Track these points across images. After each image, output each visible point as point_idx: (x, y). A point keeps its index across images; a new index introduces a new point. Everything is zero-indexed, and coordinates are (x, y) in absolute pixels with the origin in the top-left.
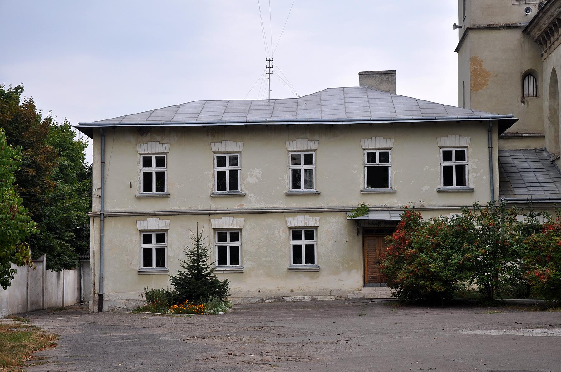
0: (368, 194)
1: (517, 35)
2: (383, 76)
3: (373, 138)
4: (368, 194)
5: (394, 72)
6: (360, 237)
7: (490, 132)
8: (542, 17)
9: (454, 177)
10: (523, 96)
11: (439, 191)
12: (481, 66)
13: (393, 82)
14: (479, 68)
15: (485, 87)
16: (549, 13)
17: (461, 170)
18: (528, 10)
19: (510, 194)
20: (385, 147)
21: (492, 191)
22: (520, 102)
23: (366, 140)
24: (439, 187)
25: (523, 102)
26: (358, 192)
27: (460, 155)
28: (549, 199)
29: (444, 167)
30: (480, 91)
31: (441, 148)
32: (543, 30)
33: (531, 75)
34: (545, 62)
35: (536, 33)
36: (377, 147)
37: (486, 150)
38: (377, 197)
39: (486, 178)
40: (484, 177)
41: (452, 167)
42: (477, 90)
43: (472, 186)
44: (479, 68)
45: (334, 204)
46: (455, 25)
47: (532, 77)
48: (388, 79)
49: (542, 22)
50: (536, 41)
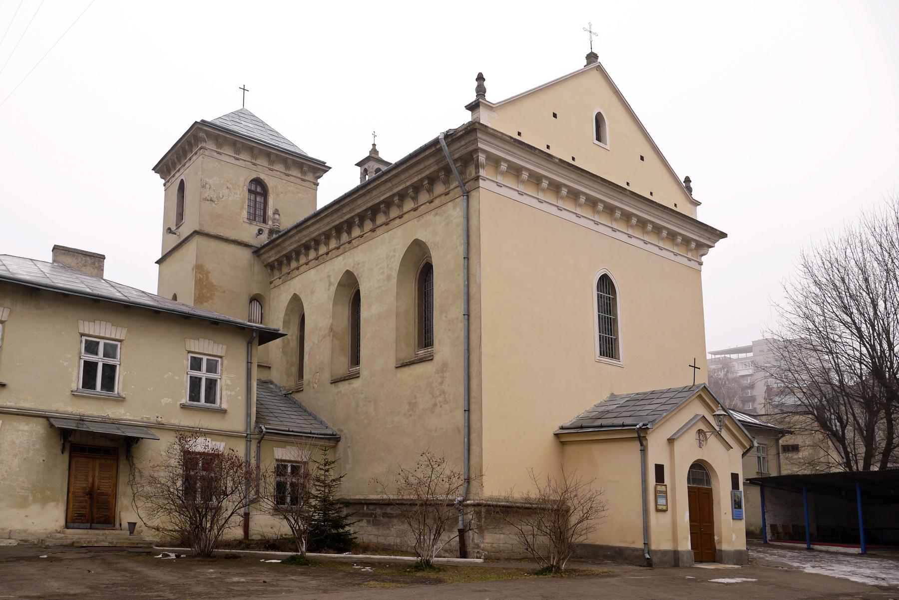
0: (83, 397)
1: (245, 255)
2: (88, 259)
3: (97, 322)
4: (83, 397)
5: (102, 257)
8: (291, 237)
13: (101, 269)
16: (304, 233)
20: (113, 336)
23: (86, 323)
26: (68, 393)
30: (205, 304)
32: (284, 252)
34: (276, 289)
36: (102, 335)
38: (96, 403)
41: (200, 379)
42: (202, 303)
45: (27, 404)
46: (169, 229)
48: (93, 264)
49: (288, 243)
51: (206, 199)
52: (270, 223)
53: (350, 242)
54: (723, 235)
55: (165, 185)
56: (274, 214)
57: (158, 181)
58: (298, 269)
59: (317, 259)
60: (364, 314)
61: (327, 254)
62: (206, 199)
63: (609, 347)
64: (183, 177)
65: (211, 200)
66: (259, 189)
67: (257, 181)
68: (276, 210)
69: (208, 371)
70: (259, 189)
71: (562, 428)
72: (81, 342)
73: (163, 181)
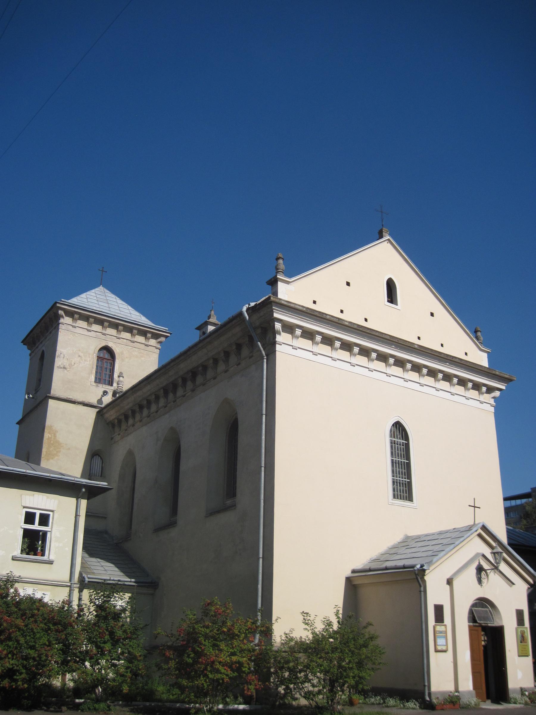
9: (34, 543)
11: (14, 559)
12: (55, 436)
14: (53, 437)
15: (56, 458)
16: (139, 393)
18: (105, 393)
19: (89, 571)
27: (44, 520)
31: (24, 507)
40: (67, 549)
43: (52, 558)
44: (53, 437)
47: (99, 458)
50: (108, 424)
51: (59, 367)
52: (115, 385)
53: (174, 401)
55: (30, 355)
56: (119, 377)
57: (25, 351)
58: (133, 425)
59: (149, 416)
60: (184, 467)
61: (157, 412)
62: (59, 367)
63: (403, 489)
64: (44, 348)
65: (64, 368)
66: (107, 356)
67: (107, 349)
68: (121, 373)
69: (40, 524)
70: (107, 356)
71: (354, 571)
73: (29, 352)
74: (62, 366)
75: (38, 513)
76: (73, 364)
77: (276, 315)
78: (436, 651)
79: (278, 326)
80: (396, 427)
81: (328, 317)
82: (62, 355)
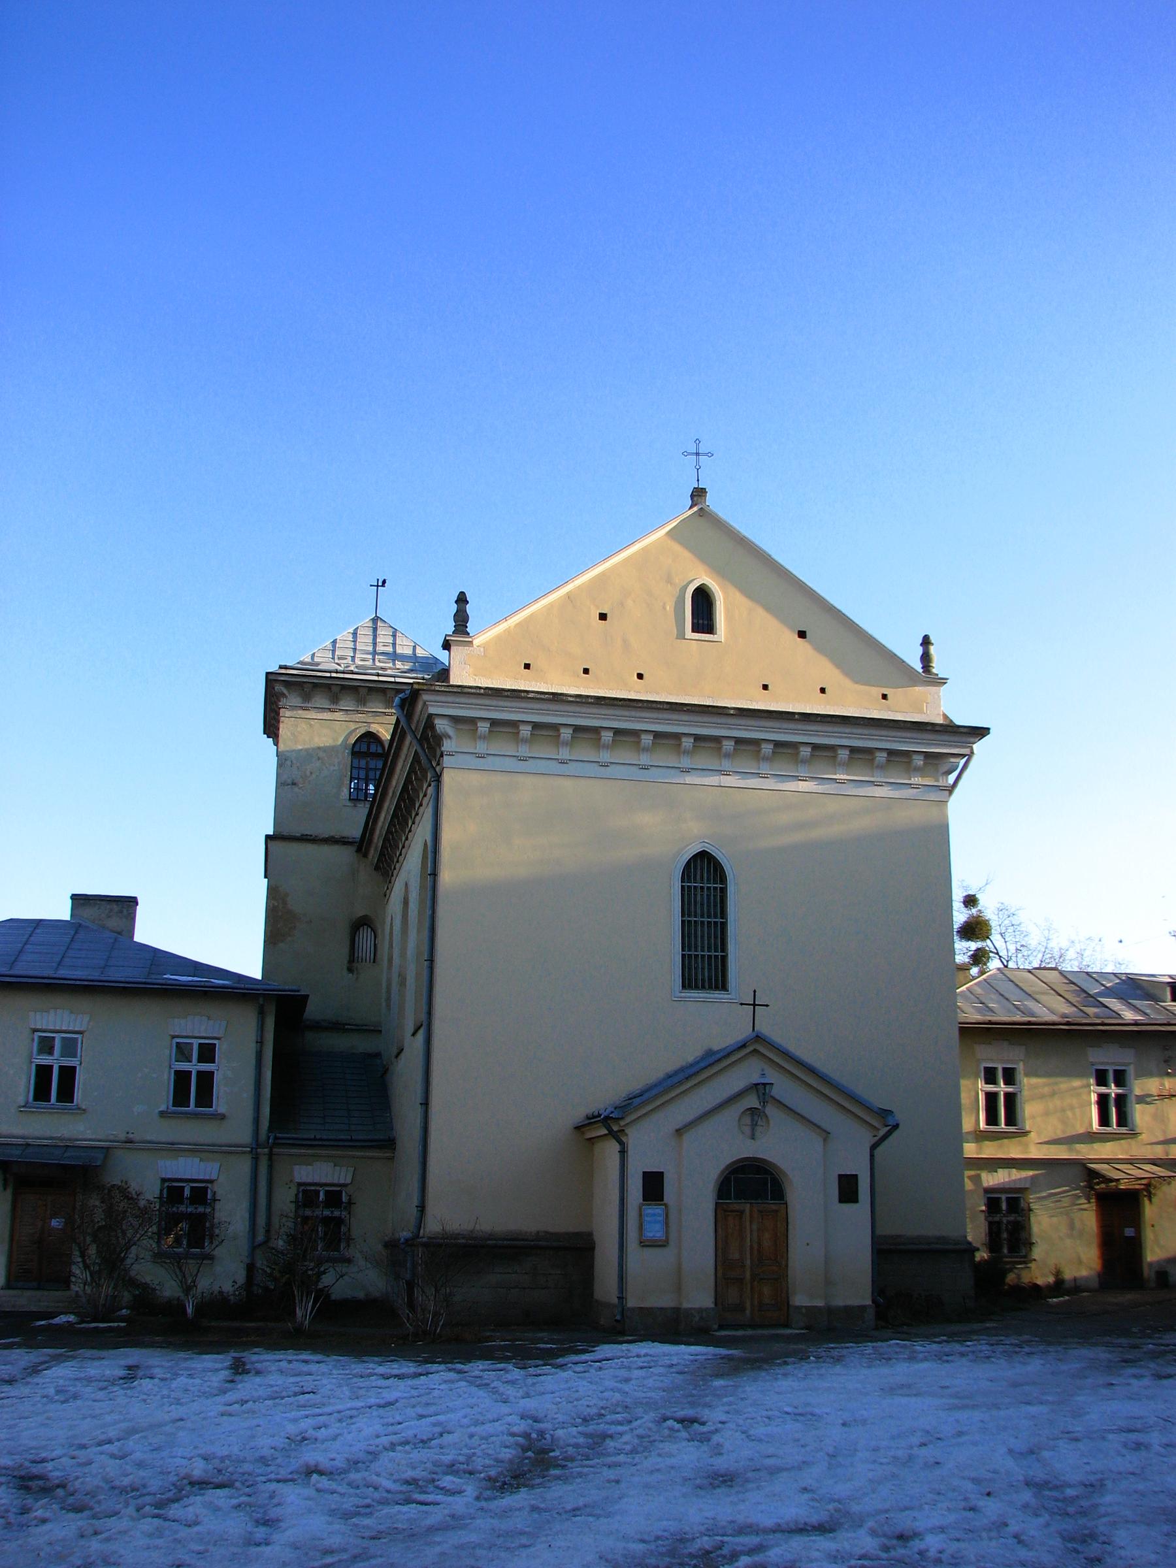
1: (344, 855)
5: (132, 902)
6: (9, 1191)
7: (262, 1013)
9: (192, 1090)
10: (352, 959)
11: (162, 1114)
12: (285, 903)
17: (206, 1080)
21: (257, 1121)
22: (345, 970)
24: (163, 1108)
25: (350, 970)
27: (207, 1053)
28: (351, 1140)
29: (177, 1073)
31: (173, 1037)
33: (369, 926)
35: (373, 854)
37: (252, 1047)
39: (247, 1095)
43: (222, 1109)
48: (121, 912)
54: (980, 732)
65: (294, 784)
71: (588, 1118)
72: (33, 1040)
74: (289, 781)
75: (196, 1043)
76: (308, 773)
77: (432, 710)
78: (645, 1244)
79: (441, 725)
80: (702, 861)
81: (530, 695)
82: (288, 763)
